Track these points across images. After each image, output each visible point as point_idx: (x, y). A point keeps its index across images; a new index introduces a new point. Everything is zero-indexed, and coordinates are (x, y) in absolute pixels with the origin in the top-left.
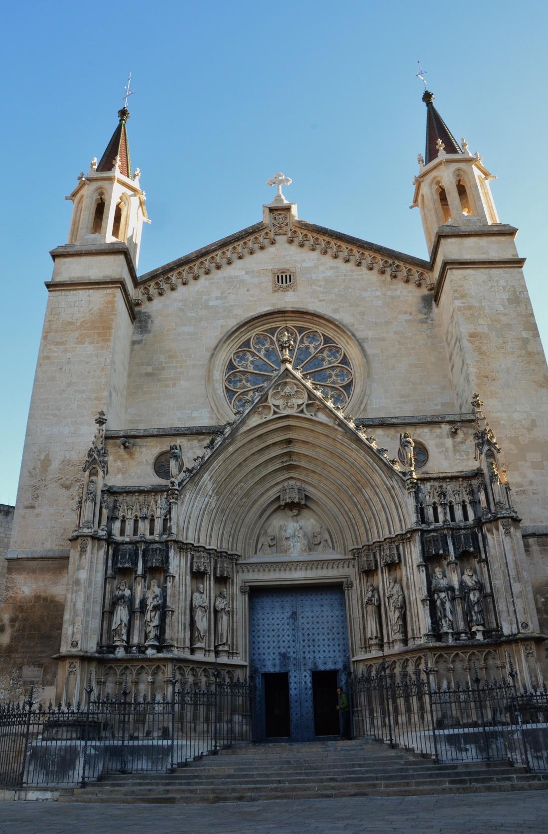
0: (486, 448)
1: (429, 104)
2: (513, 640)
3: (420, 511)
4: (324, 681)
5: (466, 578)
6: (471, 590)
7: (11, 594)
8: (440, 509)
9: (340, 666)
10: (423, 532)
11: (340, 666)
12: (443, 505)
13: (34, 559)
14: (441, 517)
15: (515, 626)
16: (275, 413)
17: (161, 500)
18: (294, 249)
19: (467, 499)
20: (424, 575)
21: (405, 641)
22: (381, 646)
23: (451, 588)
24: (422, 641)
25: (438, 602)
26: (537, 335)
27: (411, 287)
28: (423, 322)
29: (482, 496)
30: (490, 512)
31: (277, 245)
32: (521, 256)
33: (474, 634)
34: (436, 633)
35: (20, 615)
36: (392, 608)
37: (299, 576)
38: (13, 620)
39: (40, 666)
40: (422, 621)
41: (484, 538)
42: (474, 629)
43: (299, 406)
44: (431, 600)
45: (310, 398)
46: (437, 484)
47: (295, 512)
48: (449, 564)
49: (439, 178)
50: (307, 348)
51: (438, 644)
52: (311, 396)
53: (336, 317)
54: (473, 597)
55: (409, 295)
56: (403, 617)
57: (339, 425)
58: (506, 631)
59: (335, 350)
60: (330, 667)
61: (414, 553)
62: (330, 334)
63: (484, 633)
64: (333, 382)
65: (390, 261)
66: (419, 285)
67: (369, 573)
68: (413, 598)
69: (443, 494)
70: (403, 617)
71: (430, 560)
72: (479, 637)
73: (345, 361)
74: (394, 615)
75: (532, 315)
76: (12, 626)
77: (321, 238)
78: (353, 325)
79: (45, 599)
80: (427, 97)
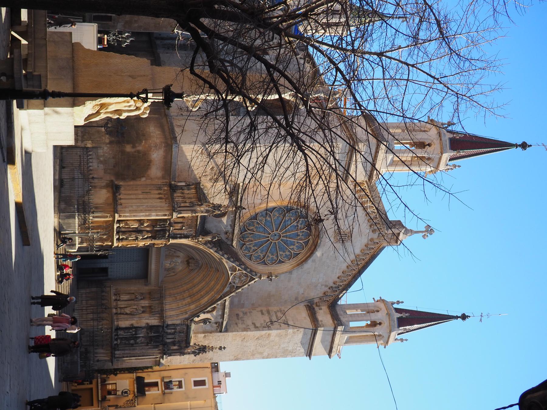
0: (197, 351)
1: (457, 317)
2: (113, 356)
3: (174, 325)
4: (105, 270)
5: (140, 339)
6: (135, 341)
7: (153, 148)
8: (173, 331)
9: (109, 277)
10: (163, 326)
11: (109, 277)
12: (175, 332)
13: (171, 159)
14: (169, 331)
15: (118, 356)
16: (231, 274)
17: (193, 233)
18: (365, 241)
19: (177, 340)
20: (144, 325)
21: (116, 314)
22: (116, 300)
23: (136, 334)
24: (116, 323)
25: (131, 331)
26: (263, 358)
27: (321, 295)
28: (296, 299)
29: (175, 347)
30: (168, 350)
31: (371, 233)
32: (312, 357)
33: (116, 340)
34: (118, 329)
35: (141, 155)
36: (131, 310)
37: (153, 266)
38: (139, 152)
39: (114, 167)
40: (124, 323)
41: (157, 347)
42: (119, 341)
43: (234, 282)
44: (132, 327)
45: (237, 287)
46: (185, 330)
47: (186, 263)
48: (148, 333)
49: (382, 325)
50: (294, 245)
51: (114, 330)
52: (238, 288)
53: (310, 261)
54: (132, 342)
55: (315, 294)
56: (127, 314)
57: (221, 296)
58: (117, 352)
59: (290, 257)
60: (109, 273)
61: (154, 321)
62: (300, 256)
63: (117, 344)
64: (268, 256)
65: (340, 288)
66: (320, 298)
67: (150, 295)
68: (135, 319)
69: (180, 332)
70: (127, 314)
71: (150, 328)
72: (115, 342)
73: (281, 262)
74: (128, 311)
75: (276, 357)
76: (135, 152)
77: (368, 257)
78: (302, 268)
79: (149, 165)
80: (464, 317)
